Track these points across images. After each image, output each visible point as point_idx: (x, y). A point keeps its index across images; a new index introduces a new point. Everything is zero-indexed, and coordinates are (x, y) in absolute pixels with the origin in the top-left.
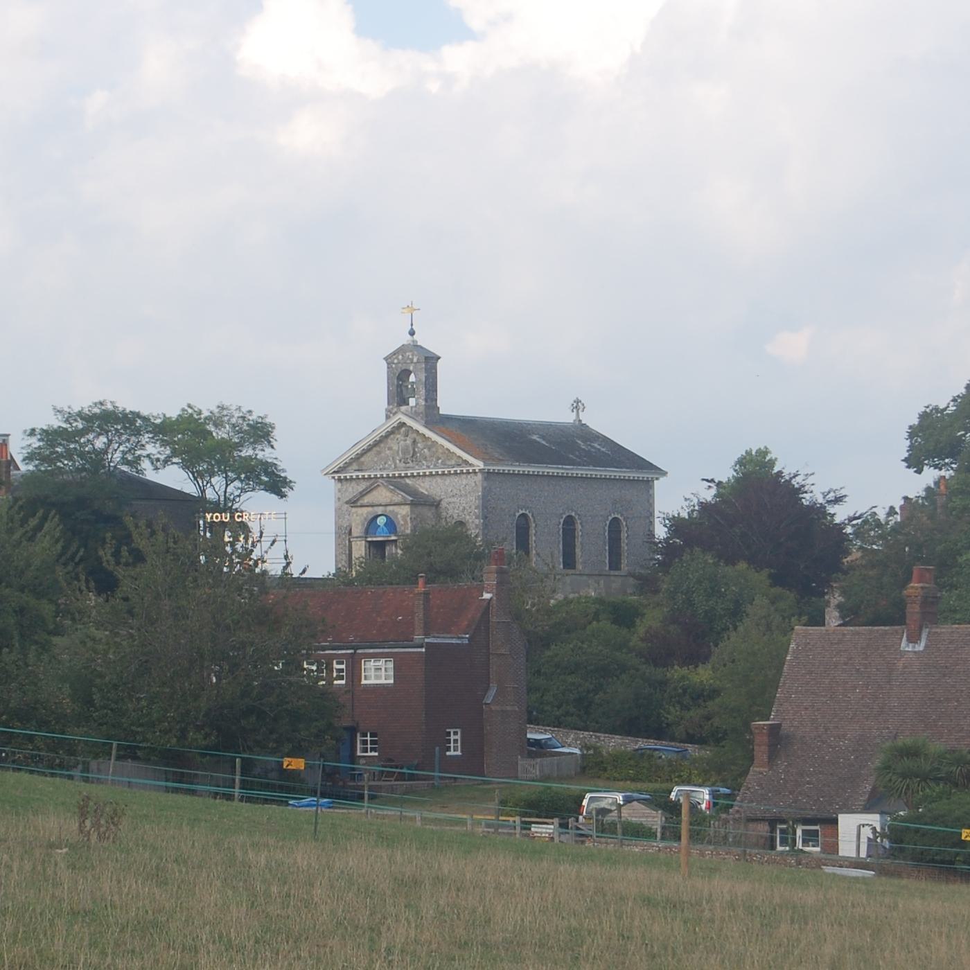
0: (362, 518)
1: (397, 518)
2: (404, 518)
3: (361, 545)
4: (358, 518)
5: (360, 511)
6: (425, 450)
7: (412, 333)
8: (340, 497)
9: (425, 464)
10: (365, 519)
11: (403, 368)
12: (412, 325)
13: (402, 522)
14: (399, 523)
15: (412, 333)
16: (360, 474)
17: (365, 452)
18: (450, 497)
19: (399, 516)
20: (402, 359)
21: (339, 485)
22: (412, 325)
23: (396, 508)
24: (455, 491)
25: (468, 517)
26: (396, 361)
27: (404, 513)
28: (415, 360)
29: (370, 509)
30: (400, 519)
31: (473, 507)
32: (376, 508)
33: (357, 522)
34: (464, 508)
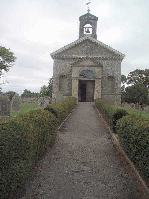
1: (95, 72)
2: (98, 72)
4: (76, 70)
5: (77, 68)
10: (79, 71)
13: (97, 73)
14: (96, 73)
15: (89, 11)
17: (70, 49)
19: (96, 71)
20: (87, 18)
21: (56, 60)
23: (95, 68)
24: (109, 65)
26: (84, 18)
27: (98, 70)
28: (93, 19)
29: (82, 68)
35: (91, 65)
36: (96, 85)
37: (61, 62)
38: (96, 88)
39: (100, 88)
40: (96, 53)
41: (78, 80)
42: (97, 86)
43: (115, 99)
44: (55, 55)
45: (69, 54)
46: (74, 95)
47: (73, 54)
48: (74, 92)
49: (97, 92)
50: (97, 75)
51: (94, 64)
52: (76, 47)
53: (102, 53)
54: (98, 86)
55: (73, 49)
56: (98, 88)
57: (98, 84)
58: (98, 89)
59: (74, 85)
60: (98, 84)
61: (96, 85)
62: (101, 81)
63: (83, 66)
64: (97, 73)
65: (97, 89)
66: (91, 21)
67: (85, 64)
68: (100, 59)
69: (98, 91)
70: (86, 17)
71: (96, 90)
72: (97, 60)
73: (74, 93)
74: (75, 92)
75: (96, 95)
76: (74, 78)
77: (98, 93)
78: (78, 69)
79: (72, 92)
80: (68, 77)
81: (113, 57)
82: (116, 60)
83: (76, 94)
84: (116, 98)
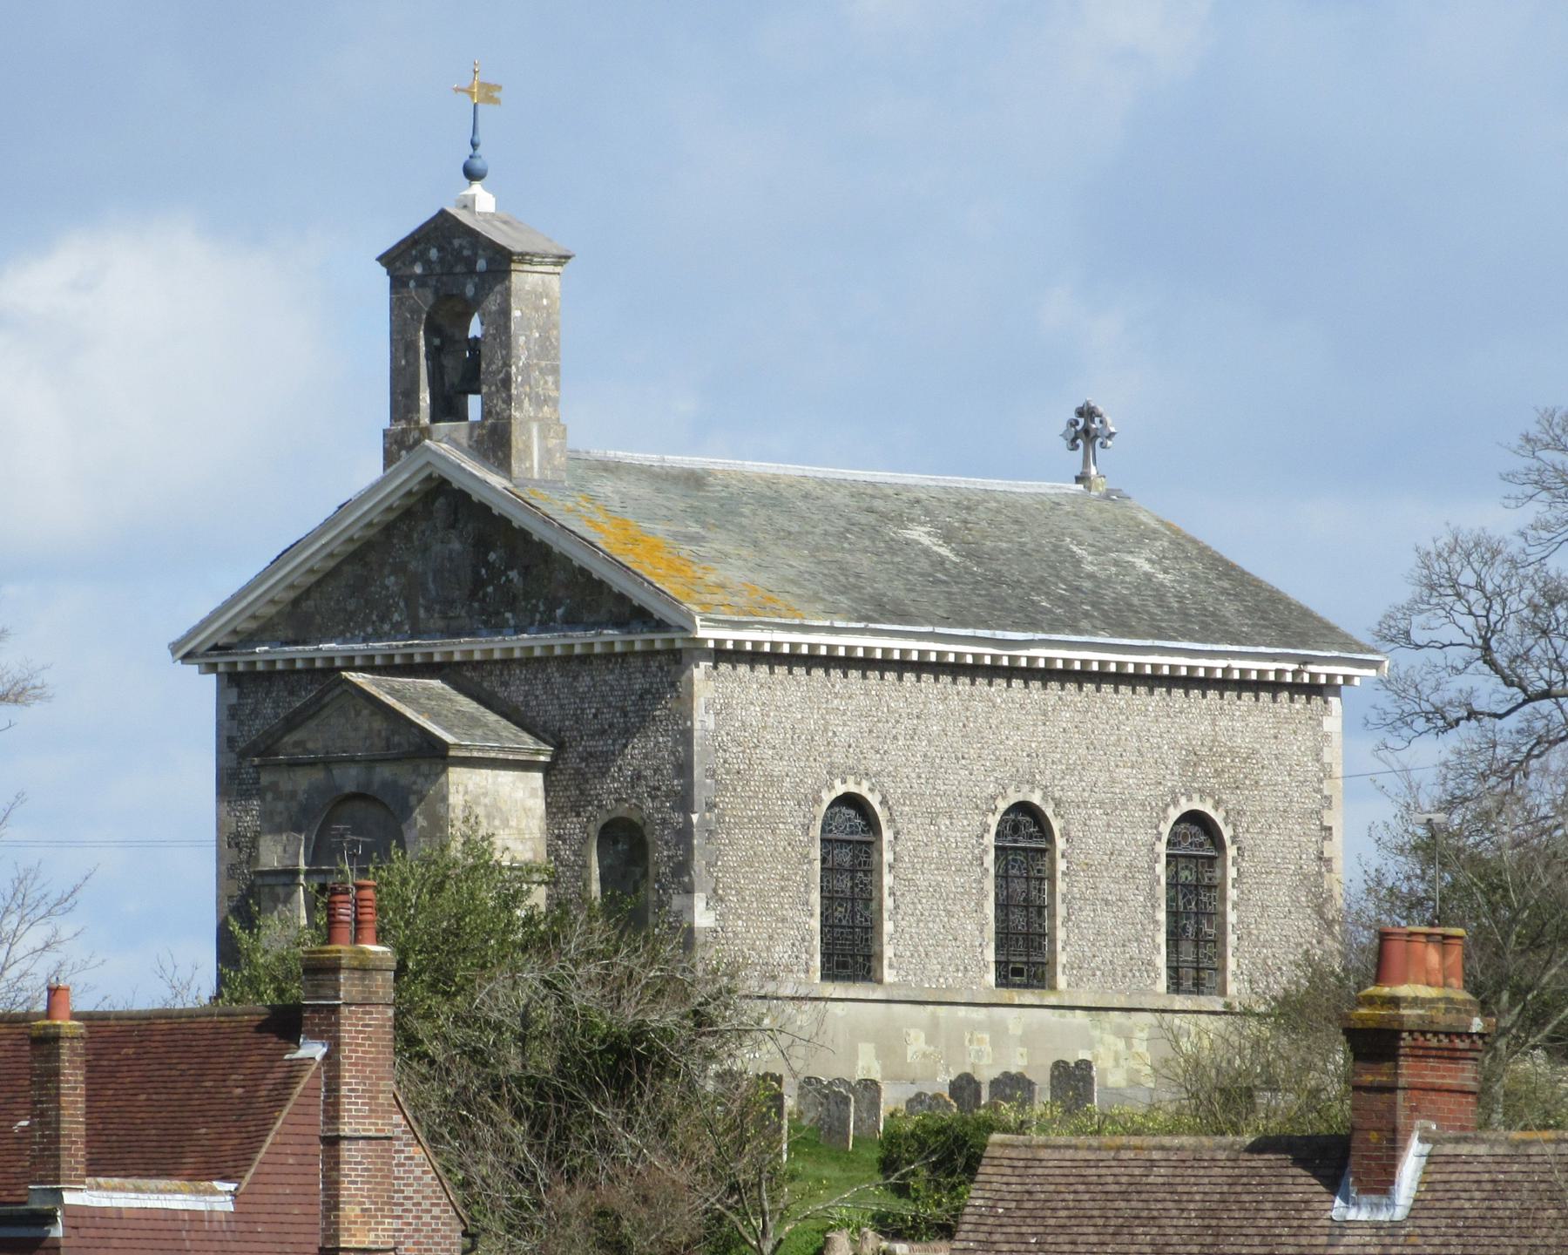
4: (280, 806)
6: (513, 574)
8: (235, 733)
9: (512, 622)
12: (474, 145)
18: (592, 736)
34: (638, 776)
53: (552, 604)
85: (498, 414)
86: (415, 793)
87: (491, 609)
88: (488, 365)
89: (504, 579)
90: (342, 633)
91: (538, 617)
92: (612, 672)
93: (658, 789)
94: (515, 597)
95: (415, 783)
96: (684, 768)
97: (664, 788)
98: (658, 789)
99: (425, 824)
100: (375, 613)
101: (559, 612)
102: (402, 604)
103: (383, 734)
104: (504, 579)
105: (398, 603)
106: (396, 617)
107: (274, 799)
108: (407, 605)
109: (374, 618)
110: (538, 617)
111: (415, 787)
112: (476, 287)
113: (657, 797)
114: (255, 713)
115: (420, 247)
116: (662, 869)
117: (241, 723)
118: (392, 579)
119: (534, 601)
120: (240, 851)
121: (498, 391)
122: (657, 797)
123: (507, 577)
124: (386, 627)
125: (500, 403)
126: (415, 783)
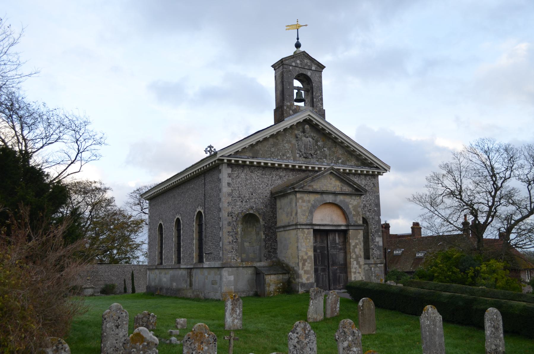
0: (310, 205)
1: (348, 208)
2: (355, 208)
3: (308, 233)
4: (305, 204)
7: (298, 45)
8: (230, 182)
9: (326, 162)
11: (300, 72)
12: (298, 39)
13: (353, 213)
14: (351, 213)
15: (298, 45)
16: (255, 161)
19: (350, 206)
20: (301, 64)
22: (298, 39)
23: (347, 199)
25: (368, 213)
29: (318, 196)
30: (352, 209)
31: (373, 205)
32: (324, 196)
33: (304, 208)
35: (338, 190)
36: (353, 244)
37: (243, 176)
38: (354, 250)
39: (360, 249)
40: (326, 158)
41: (312, 230)
42: (355, 247)
43: (372, 275)
44: (230, 156)
45: (264, 157)
46: (306, 272)
47: (272, 155)
48: (304, 264)
49: (355, 262)
50: (354, 215)
51: (344, 188)
52: (279, 138)
53: (338, 159)
54: (356, 244)
55: (271, 141)
56: (357, 250)
57: (357, 241)
58: (357, 253)
59: (304, 244)
60: (357, 241)
61: (353, 242)
62: (361, 232)
63: (322, 193)
64: (353, 213)
65: (355, 253)
66: (309, 74)
67: (324, 189)
68: (356, 174)
69: (357, 259)
70: (298, 62)
71: (354, 256)
72: (352, 178)
73: (305, 269)
74: (306, 264)
75: (355, 270)
76: (302, 225)
77: (358, 263)
78: (309, 201)
79: (301, 265)
80: (263, 220)
81: (365, 170)
82: (368, 178)
83: (309, 269)
84: (375, 273)
85: (319, 107)
86: (351, 204)
87: (319, 157)
88: (316, 94)
89: (323, 150)
90: (270, 157)
91: (333, 161)
92: (356, 178)
93: (371, 210)
94: (326, 155)
95: (351, 201)
96: (378, 205)
97: (372, 210)
98: (371, 210)
99: (355, 213)
100: (281, 153)
101: (340, 161)
102: (290, 152)
103: (340, 186)
104: (323, 150)
105: (289, 151)
106: (288, 155)
107: (302, 202)
108: (291, 152)
109: (281, 155)
110: (333, 161)
111: (351, 203)
112: (311, 73)
113: (370, 212)
114: (238, 177)
115: (294, 59)
116: (373, 231)
117: (233, 179)
118: (287, 144)
119: (332, 157)
120: (233, 218)
121: (319, 101)
122: (370, 212)
123: (324, 150)
124: (285, 158)
125: (320, 104)
126: (351, 201)
